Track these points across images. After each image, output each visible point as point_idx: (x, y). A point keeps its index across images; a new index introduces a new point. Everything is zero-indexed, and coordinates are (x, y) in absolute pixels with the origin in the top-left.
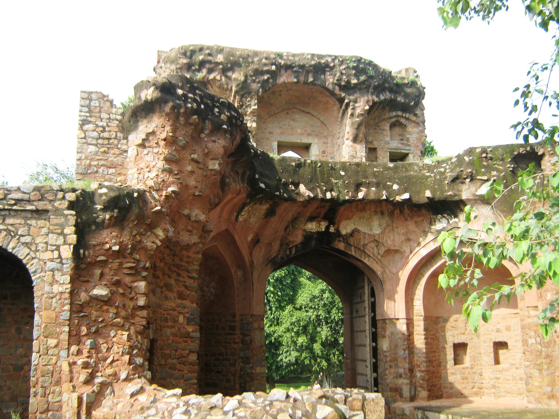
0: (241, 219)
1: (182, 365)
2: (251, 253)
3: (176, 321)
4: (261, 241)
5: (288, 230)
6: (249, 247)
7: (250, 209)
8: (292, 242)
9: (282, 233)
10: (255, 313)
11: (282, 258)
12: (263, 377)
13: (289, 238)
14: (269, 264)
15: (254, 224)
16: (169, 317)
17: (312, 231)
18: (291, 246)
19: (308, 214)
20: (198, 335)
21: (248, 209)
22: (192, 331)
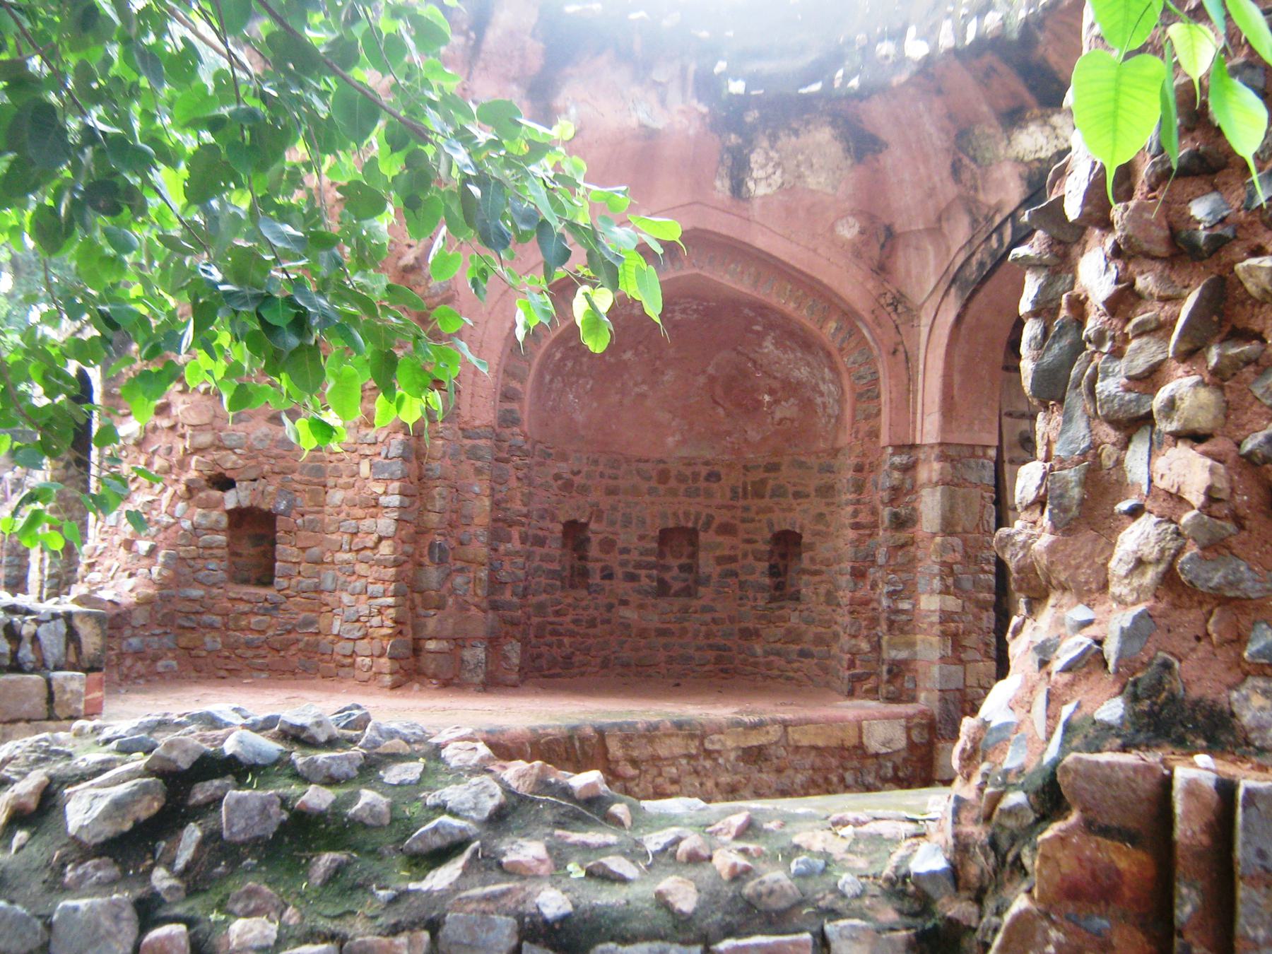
0: (758, 189)
1: (364, 566)
2: (882, 269)
3: (355, 474)
4: (898, 228)
5: (966, 176)
6: (858, 254)
7: (773, 154)
8: (998, 209)
9: (951, 190)
10: (918, 442)
11: (981, 264)
12: (932, 624)
13: (981, 197)
14: (953, 290)
15: (829, 190)
16: (341, 465)
17: (1042, 155)
18: (998, 220)
19: (985, 108)
20: (395, 500)
21: (768, 159)
22: (385, 493)
